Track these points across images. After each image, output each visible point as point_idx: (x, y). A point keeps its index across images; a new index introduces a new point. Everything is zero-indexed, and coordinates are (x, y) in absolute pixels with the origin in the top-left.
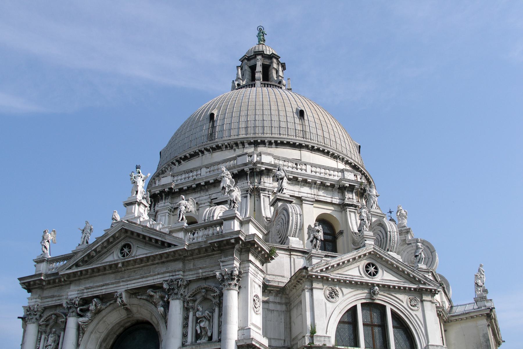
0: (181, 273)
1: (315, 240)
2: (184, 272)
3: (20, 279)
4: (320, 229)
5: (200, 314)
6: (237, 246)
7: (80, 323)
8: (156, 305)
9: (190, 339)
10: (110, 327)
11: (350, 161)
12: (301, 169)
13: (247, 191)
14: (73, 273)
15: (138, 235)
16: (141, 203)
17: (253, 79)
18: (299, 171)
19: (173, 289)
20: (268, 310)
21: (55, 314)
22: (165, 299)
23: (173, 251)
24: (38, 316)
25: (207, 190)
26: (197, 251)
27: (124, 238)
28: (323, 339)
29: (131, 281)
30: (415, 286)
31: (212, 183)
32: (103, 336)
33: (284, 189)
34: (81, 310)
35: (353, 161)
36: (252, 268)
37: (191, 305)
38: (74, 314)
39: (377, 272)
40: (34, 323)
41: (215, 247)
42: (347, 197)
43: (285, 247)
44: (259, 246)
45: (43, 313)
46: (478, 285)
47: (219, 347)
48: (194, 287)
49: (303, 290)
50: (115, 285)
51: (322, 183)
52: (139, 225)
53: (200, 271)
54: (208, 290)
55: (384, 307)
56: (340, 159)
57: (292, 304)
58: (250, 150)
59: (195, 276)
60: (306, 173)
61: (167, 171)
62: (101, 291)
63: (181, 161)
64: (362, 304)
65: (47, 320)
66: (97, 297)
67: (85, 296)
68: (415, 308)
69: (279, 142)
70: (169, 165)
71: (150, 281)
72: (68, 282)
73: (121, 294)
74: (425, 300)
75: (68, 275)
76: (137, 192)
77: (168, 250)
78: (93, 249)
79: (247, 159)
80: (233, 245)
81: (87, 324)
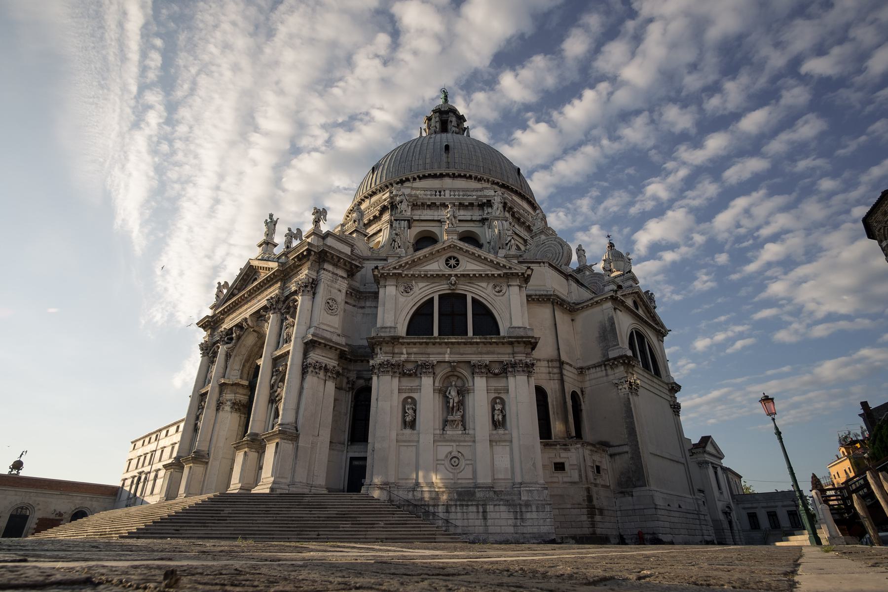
3: (197, 324)
11: (496, 180)
12: (440, 195)
19: (272, 305)
20: (363, 314)
24: (208, 350)
34: (228, 339)
36: (325, 276)
39: (458, 264)
44: (333, 255)
51: (460, 204)
55: (466, 295)
56: (485, 180)
66: (236, 326)
68: (501, 293)
69: (421, 176)
74: (510, 285)
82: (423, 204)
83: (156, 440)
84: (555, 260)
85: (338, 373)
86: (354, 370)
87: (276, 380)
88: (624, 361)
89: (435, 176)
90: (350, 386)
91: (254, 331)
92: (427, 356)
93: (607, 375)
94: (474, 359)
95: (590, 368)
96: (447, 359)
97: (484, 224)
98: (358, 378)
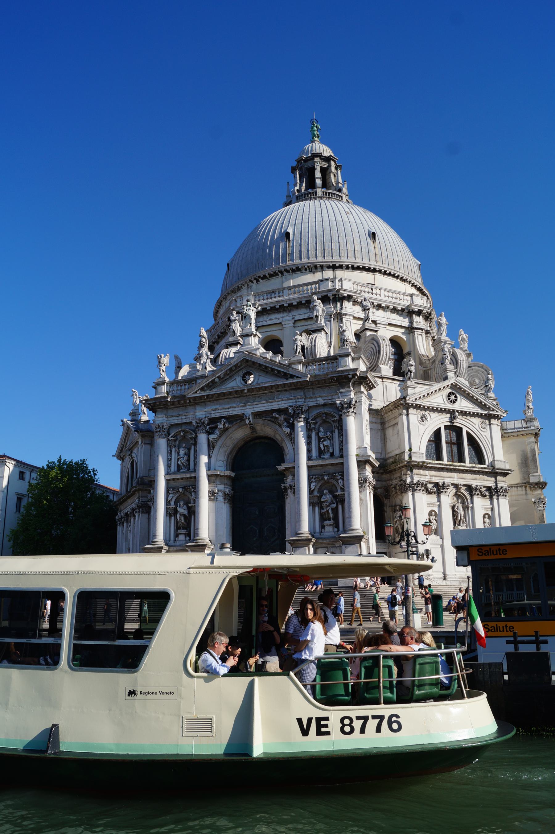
0: (303, 400)
1: (409, 373)
2: (305, 399)
4: (413, 364)
5: (323, 434)
7: (211, 439)
8: (280, 425)
11: (416, 283)
12: (376, 294)
13: (331, 316)
14: (200, 396)
15: (260, 365)
16: (257, 335)
17: (311, 184)
18: (374, 296)
21: (183, 431)
22: (291, 422)
23: (297, 382)
24: (166, 432)
25: (290, 311)
26: (317, 382)
27: (244, 367)
28: (418, 455)
29: (256, 405)
30: (486, 412)
31: (295, 305)
35: (418, 284)
37: (313, 426)
39: (456, 400)
40: (164, 438)
41: (334, 380)
42: (415, 320)
43: (379, 375)
44: (369, 380)
46: (529, 408)
47: (342, 461)
48: (314, 413)
49: (401, 414)
50: (241, 408)
51: (394, 307)
52: (278, 363)
53: (319, 399)
54: (327, 414)
55: (461, 429)
57: (387, 424)
58: (329, 273)
59: (316, 402)
61: (244, 288)
62: (229, 413)
63: (260, 279)
64: (445, 426)
65: (175, 436)
67: (213, 416)
70: (246, 282)
71: (275, 406)
72: (192, 404)
75: (195, 398)
76: (251, 324)
77: (290, 381)
78: (217, 376)
79: (330, 286)
80: (350, 379)
81: (217, 440)
87: (316, 486)
88: (542, 486)
89: (368, 270)
92: (443, 478)
93: (526, 494)
94: (474, 483)
95: (512, 487)
96: (455, 483)
97: (413, 333)
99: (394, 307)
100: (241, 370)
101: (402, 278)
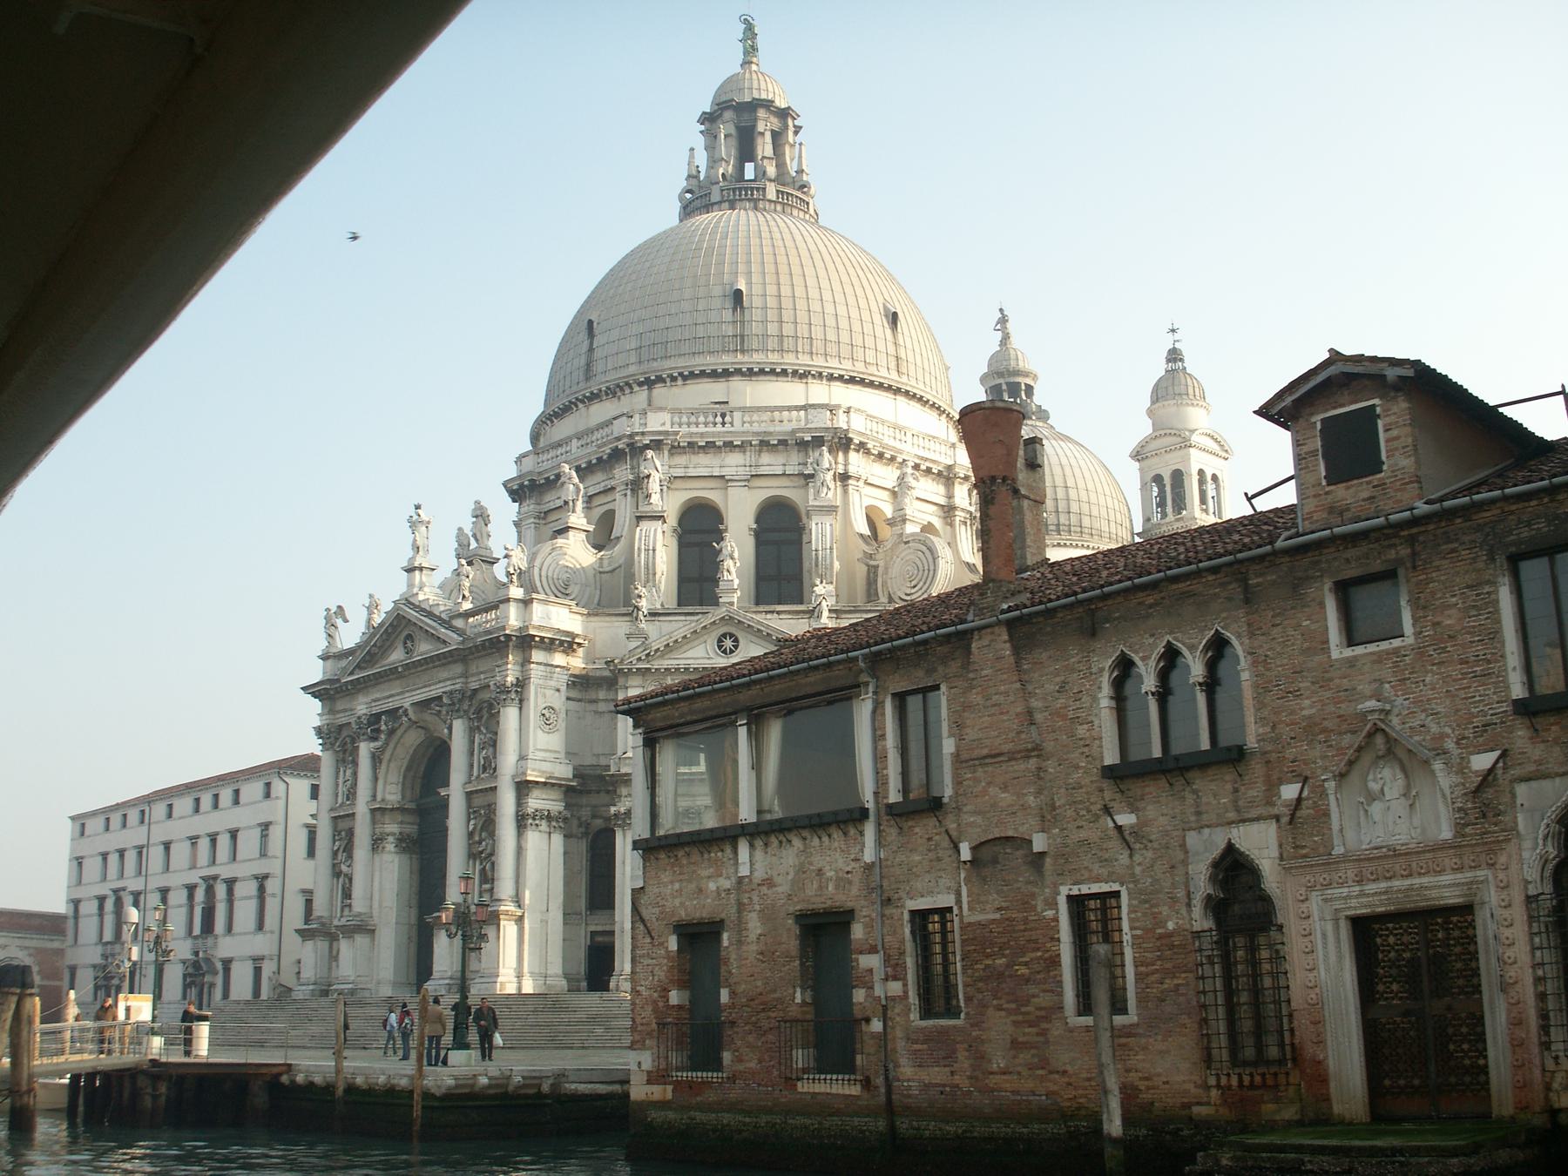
6: (511, 644)
8: (445, 722)
9: (475, 774)
10: (411, 751)
12: (723, 424)
19: (453, 704)
20: (596, 712)
24: (332, 739)
32: (405, 765)
33: (653, 495)
36: (536, 672)
38: (365, 737)
39: (736, 647)
40: (327, 750)
44: (542, 638)
45: (339, 733)
51: (761, 441)
53: (482, 676)
58: (641, 396)
60: (732, 429)
71: (435, 691)
73: (406, 710)
82: (691, 445)
83: (142, 822)
84: (921, 583)
85: (565, 820)
86: (586, 806)
89: (714, 375)
90: (582, 830)
91: (420, 727)
98: (594, 816)
99: (761, 441)
100: (401, 632)
101: (795, 373)
